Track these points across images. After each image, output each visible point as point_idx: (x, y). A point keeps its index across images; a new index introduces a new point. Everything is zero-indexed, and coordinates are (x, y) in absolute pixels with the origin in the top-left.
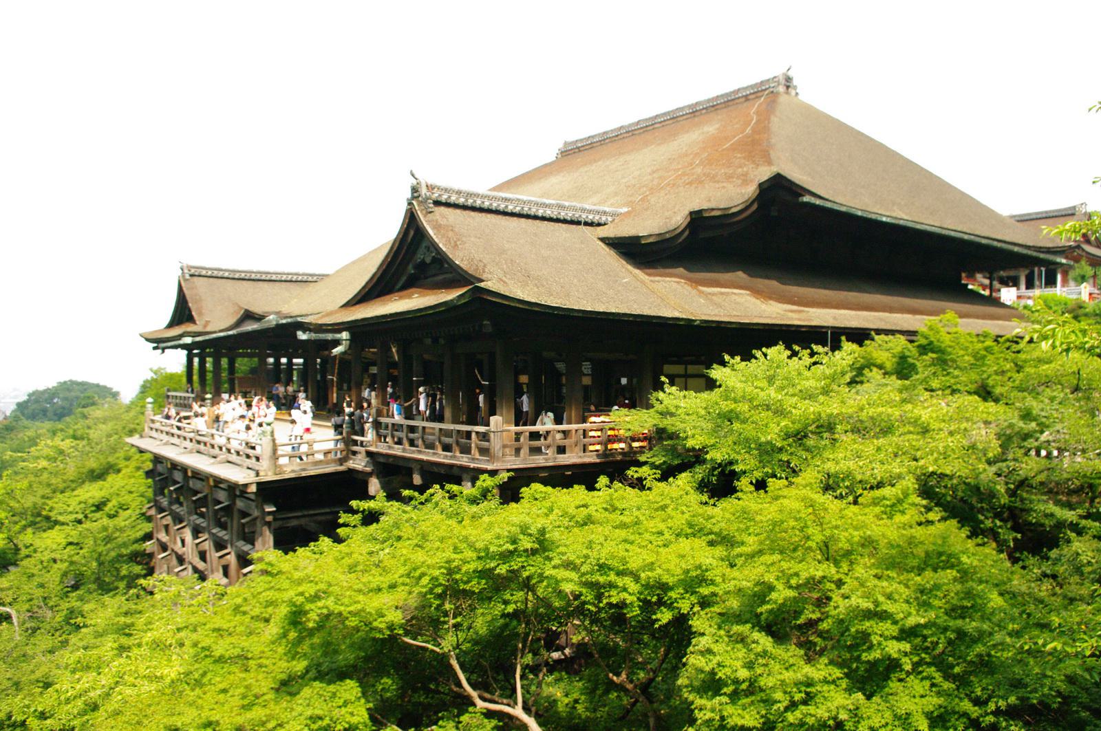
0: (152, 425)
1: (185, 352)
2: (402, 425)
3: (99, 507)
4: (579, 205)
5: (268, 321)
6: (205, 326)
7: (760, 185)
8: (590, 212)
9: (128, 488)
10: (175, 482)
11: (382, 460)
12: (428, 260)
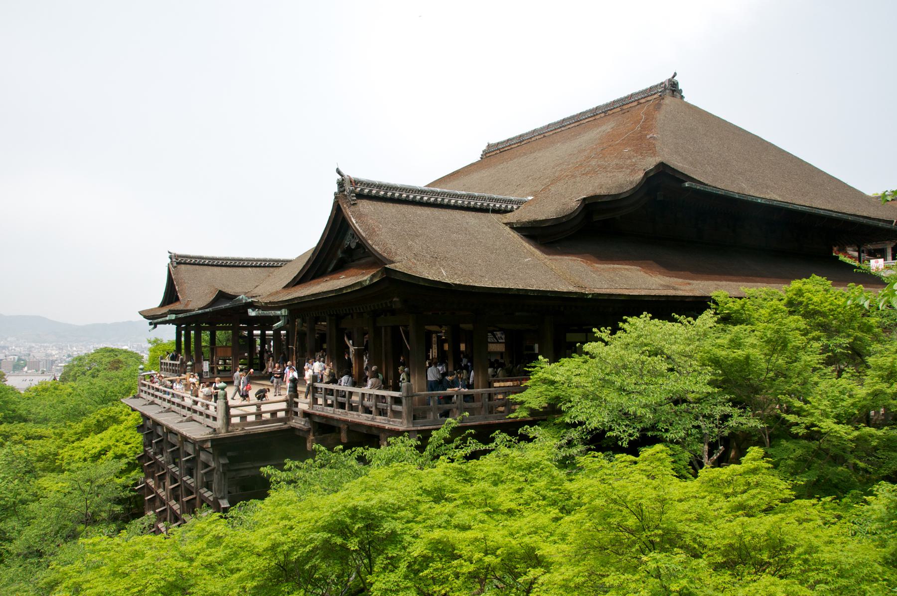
1: (175, 327)
4: (487, 195)
6: (187, 305)
8: (497, 200)
9: (126, 439)
10: (159, 436)
11: (317, 420)
12: (353, 246)
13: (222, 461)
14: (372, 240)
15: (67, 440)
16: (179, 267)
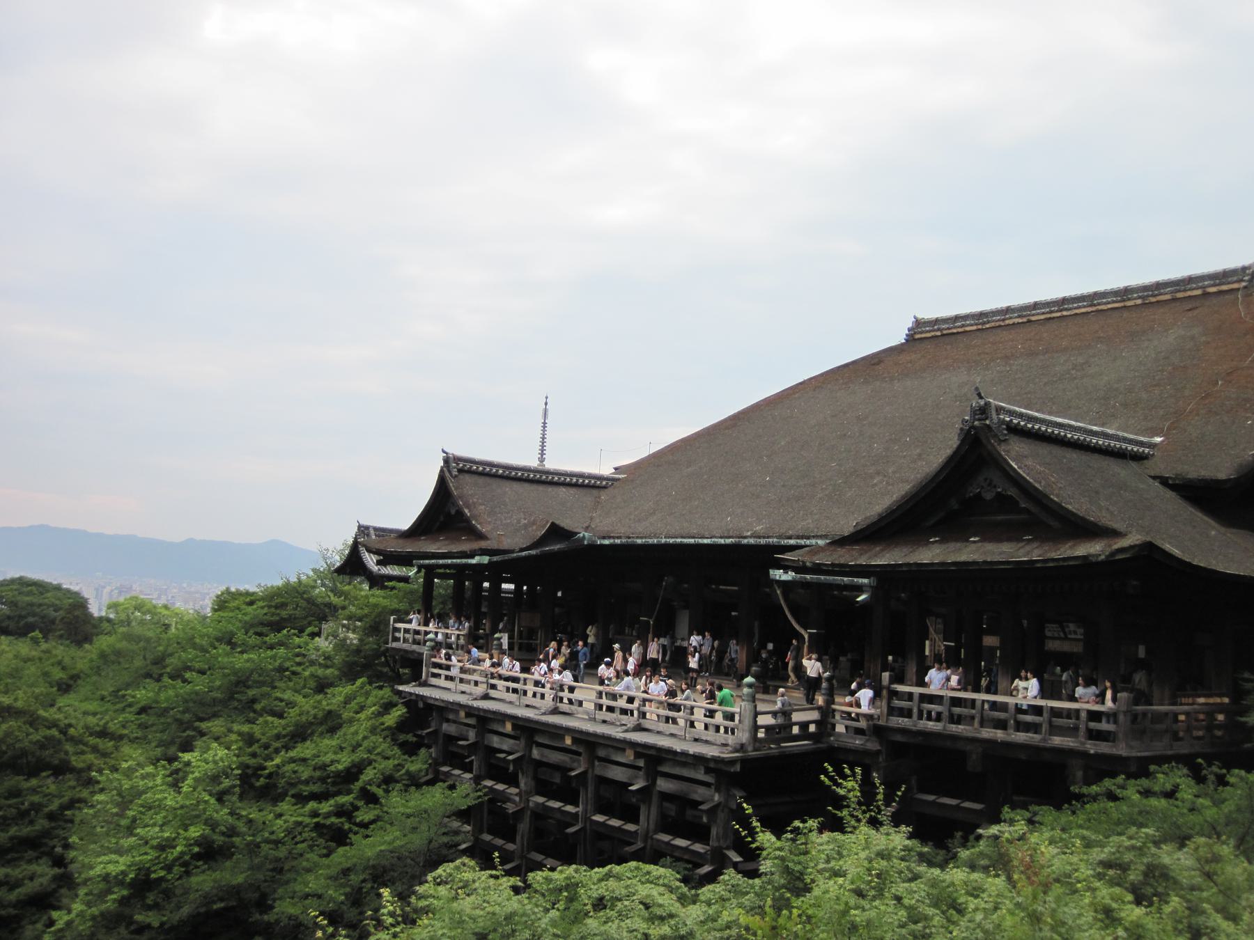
0: (436, 671)
2: (942, 697)
3: (352, 774)
4: (1121, 434)
8: (1131, 441)
11: (899, 738)
12: (988, 496)
14: (1057, 496)
15: (266, 747)
16: (461, 477)
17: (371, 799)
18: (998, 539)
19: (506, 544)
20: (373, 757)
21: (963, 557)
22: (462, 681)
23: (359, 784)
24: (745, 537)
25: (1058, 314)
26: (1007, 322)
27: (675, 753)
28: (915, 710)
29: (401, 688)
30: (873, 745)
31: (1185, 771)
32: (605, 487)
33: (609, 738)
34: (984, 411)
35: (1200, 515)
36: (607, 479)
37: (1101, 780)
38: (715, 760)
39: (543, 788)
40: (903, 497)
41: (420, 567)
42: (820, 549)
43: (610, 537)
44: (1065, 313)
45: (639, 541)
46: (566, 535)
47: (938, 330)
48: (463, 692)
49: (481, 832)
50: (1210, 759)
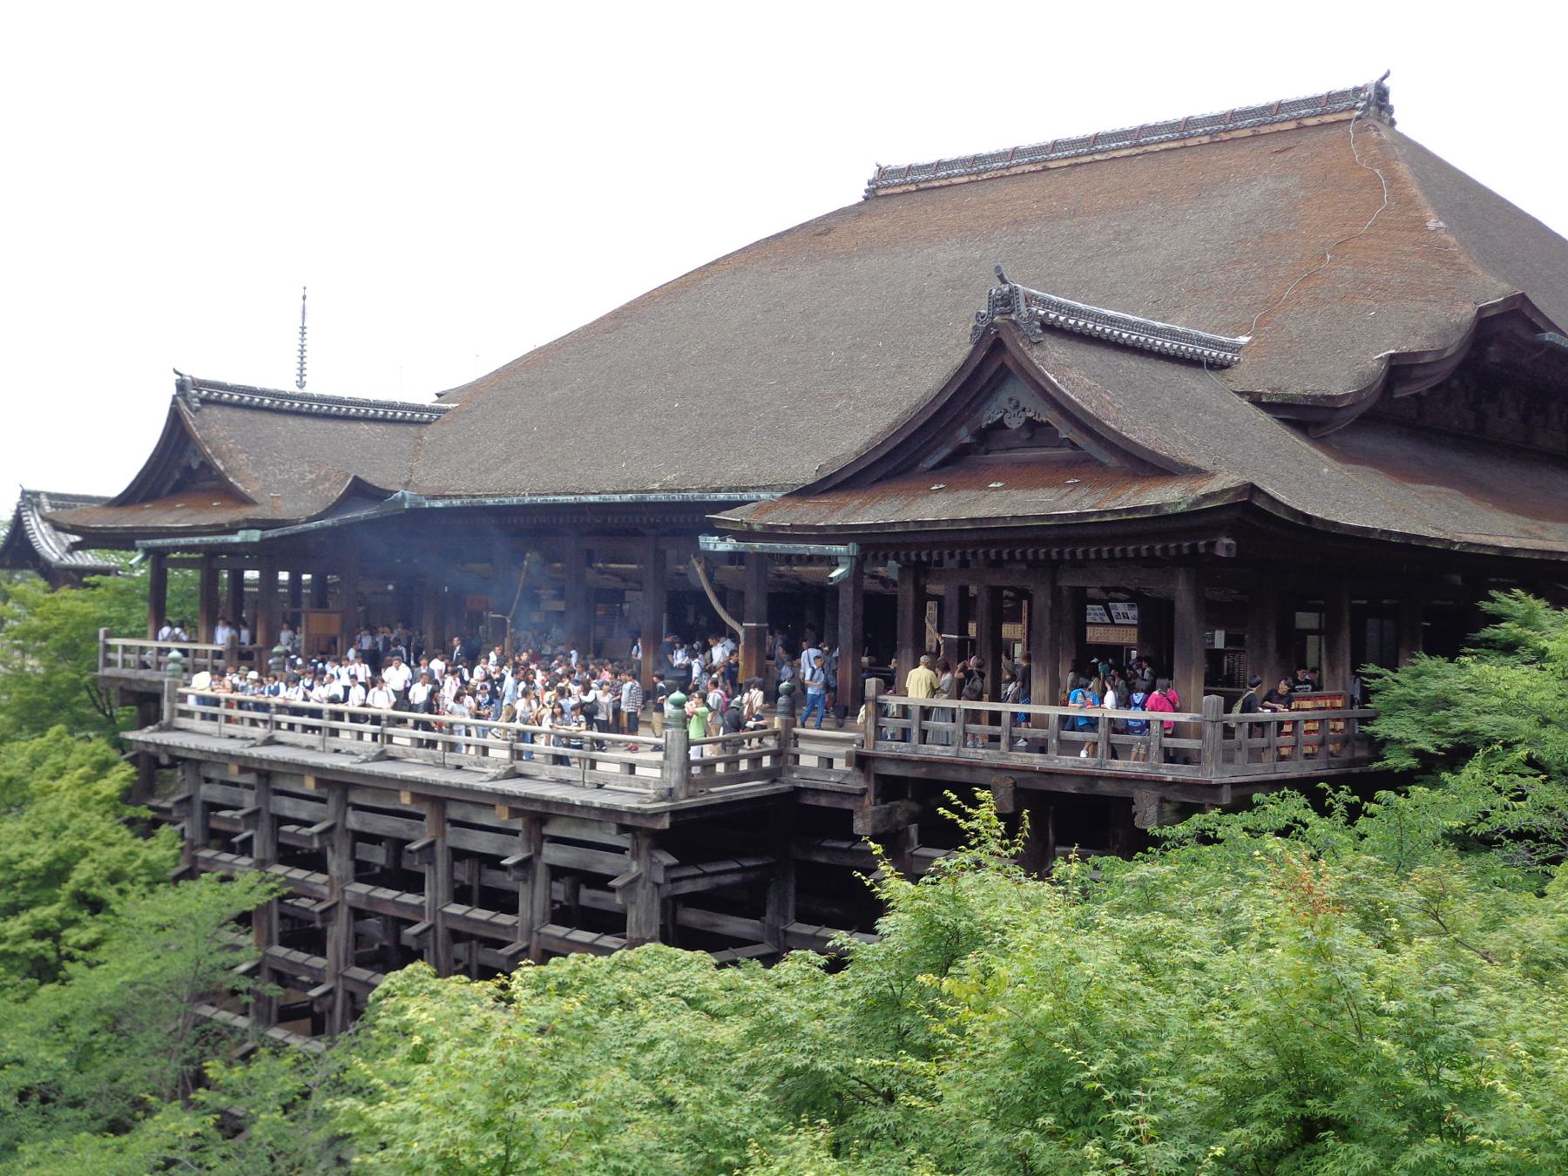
3: (55, 874)
5: (395, 502)
7: (1481, 310)
8: (1207, 343)
11: (892, 770)
12: (1014, 423)
13: (669, 860)
14: (1115, 421)
16: (206, 410)
17: (97, 907)
18: (1030, 485)
19: (285, 510)
20: (88, 844)
21: (982, 512)
22: (229, 719)
23: (69, 887)
24: (652, 491)
25: (1089, 159)
26: (1013, 170)
27: (572, 806)
28: (915, 731)
29: (131, 735)
30: (857, 783)
31: (1303, 800)
32: (428, 423)
33: (469, 790)
34: (1007, 301)
35: (1307, 446)
36: (430, 410)
37: (1188, 817)
38: (633, 813)
39: (363, 872)
40: (891, 427)
41: (148, 552)
42: (772, 506)
43: (444, 497)
44: (1098, 157)
45: (490, 502)
46: (375, 494)
47: (913, 182)
48: (232, 737)
49: (269, 943)
50: (1335, 782)
